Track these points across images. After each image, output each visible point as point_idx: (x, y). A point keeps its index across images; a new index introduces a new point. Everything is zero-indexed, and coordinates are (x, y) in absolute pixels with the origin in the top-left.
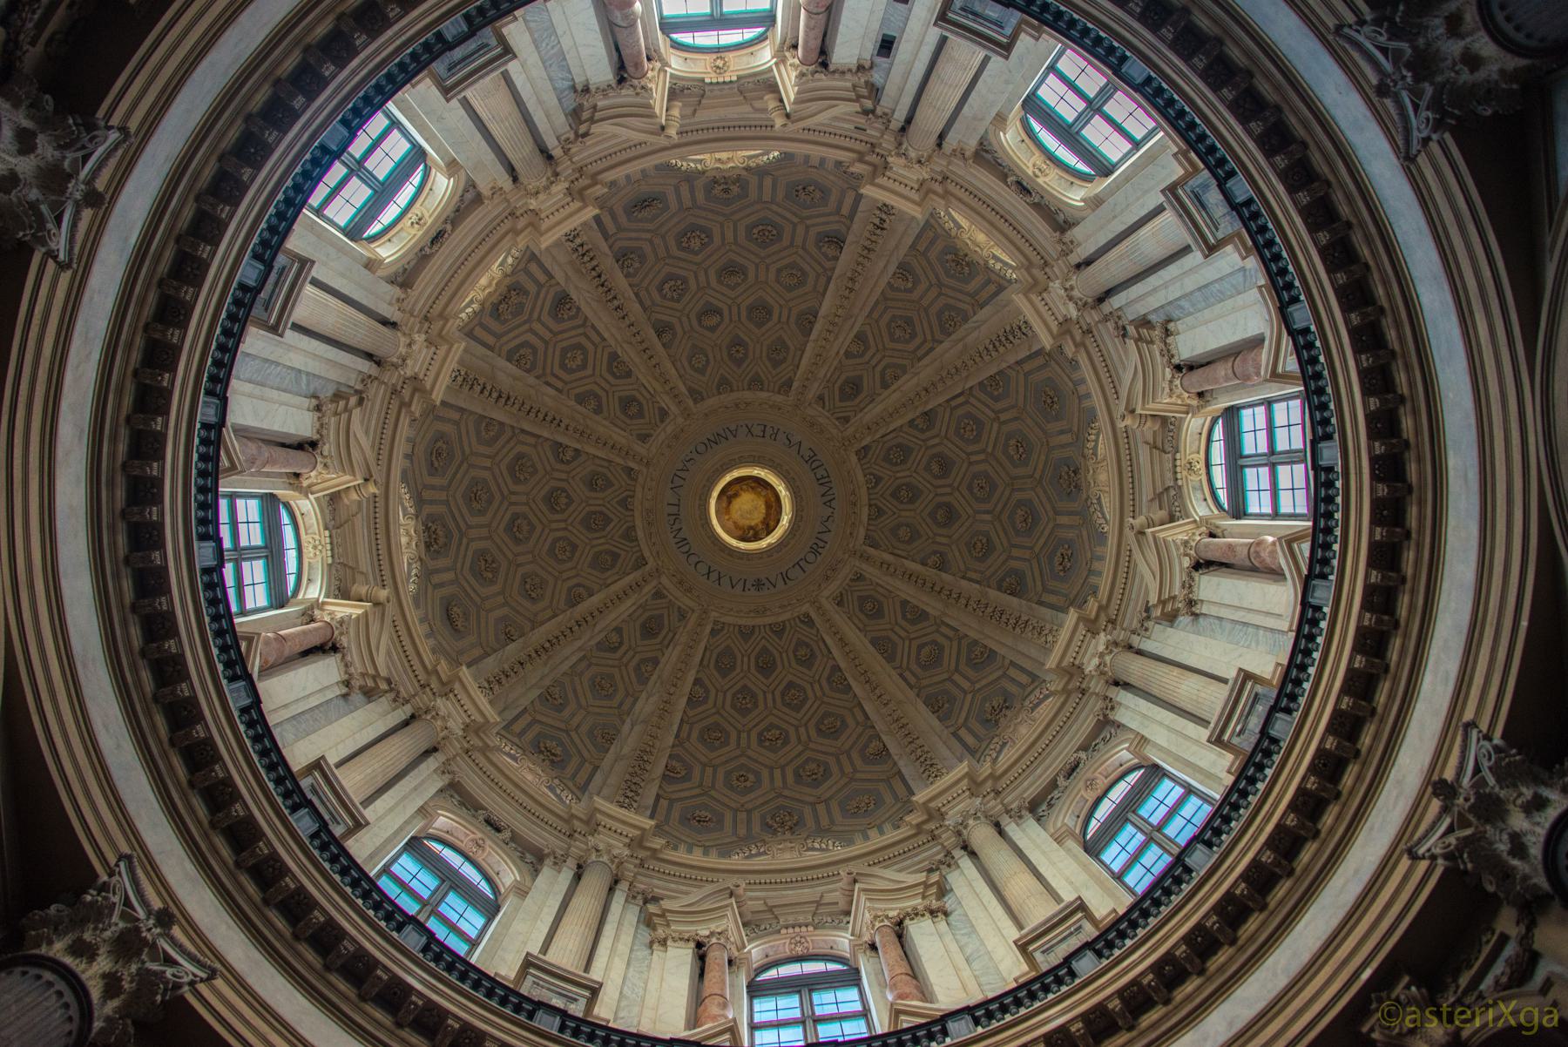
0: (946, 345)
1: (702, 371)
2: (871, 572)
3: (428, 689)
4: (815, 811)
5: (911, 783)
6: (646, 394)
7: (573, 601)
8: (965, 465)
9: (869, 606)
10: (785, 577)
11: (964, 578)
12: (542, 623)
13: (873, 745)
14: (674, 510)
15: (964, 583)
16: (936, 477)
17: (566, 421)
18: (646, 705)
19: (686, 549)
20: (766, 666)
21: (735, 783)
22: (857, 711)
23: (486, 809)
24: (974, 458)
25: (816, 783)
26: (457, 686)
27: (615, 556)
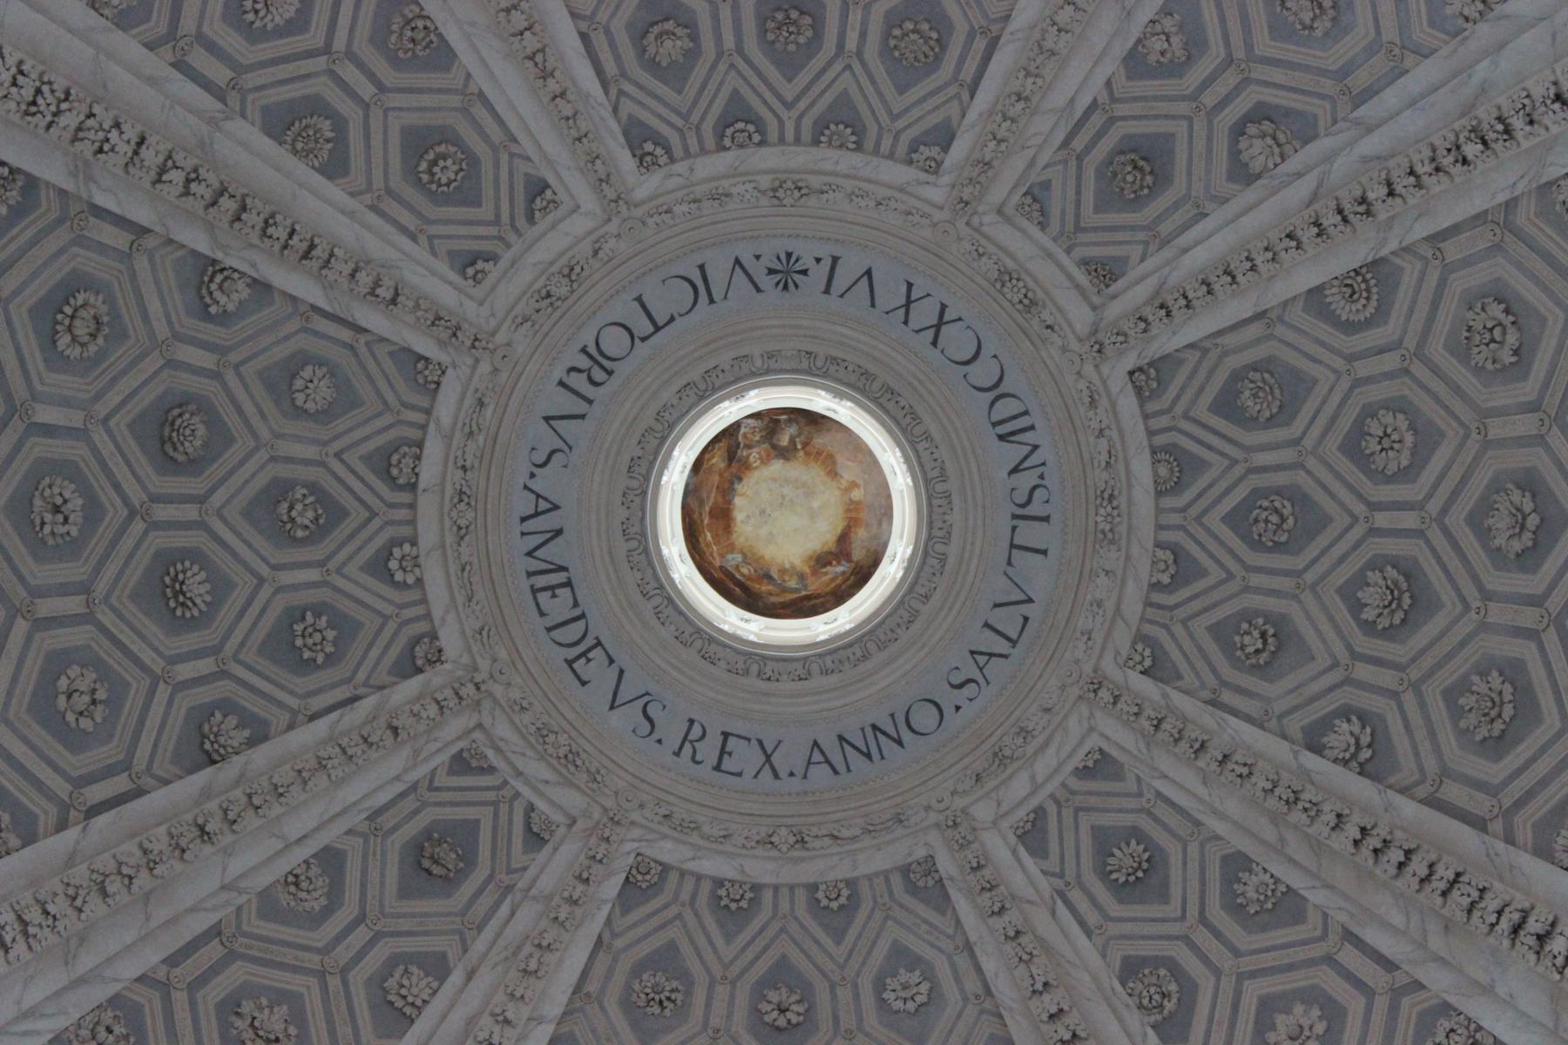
0: (130, 969)
1: (900, 956)
6: (1083, 906)
8: (101, 587)
10: (700, 287)
11: (143, 231)
12: (1480, 218)
14: (1029, 534)
15: (141, 213)
16: (195, 555)
17: (1342, 841)
19: (1005, 408)
24: (74, 604)
27: (1227, 405)
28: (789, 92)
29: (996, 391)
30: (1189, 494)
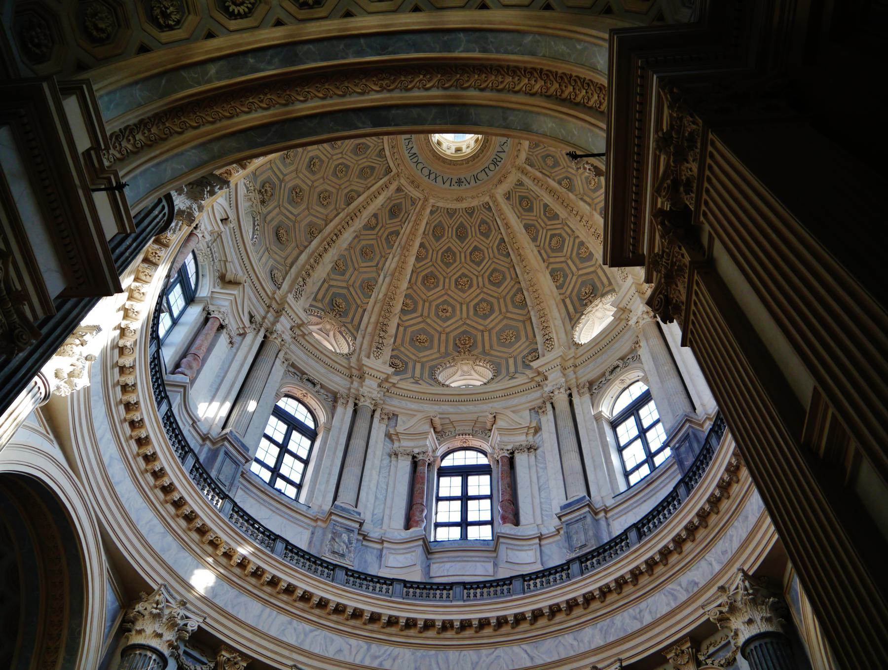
2: (527, 181)
3: (271, 309)
4: (483, 336)
5: (536, 330)
7: (350, 200)
9: (524, 204)
10: (476, 178)
11: (582, 199)
12: (331, 221)
13: (518, 296)
15: (581, 203)
18: (391, 264)
20: (462, 234)
21: (440, 313)
22: (512, 270)
23: (307, 374)
25: (485, 317)
26: (286, 306)
28: (461, 219)
29: (417, 163)
30: (377, 150)
